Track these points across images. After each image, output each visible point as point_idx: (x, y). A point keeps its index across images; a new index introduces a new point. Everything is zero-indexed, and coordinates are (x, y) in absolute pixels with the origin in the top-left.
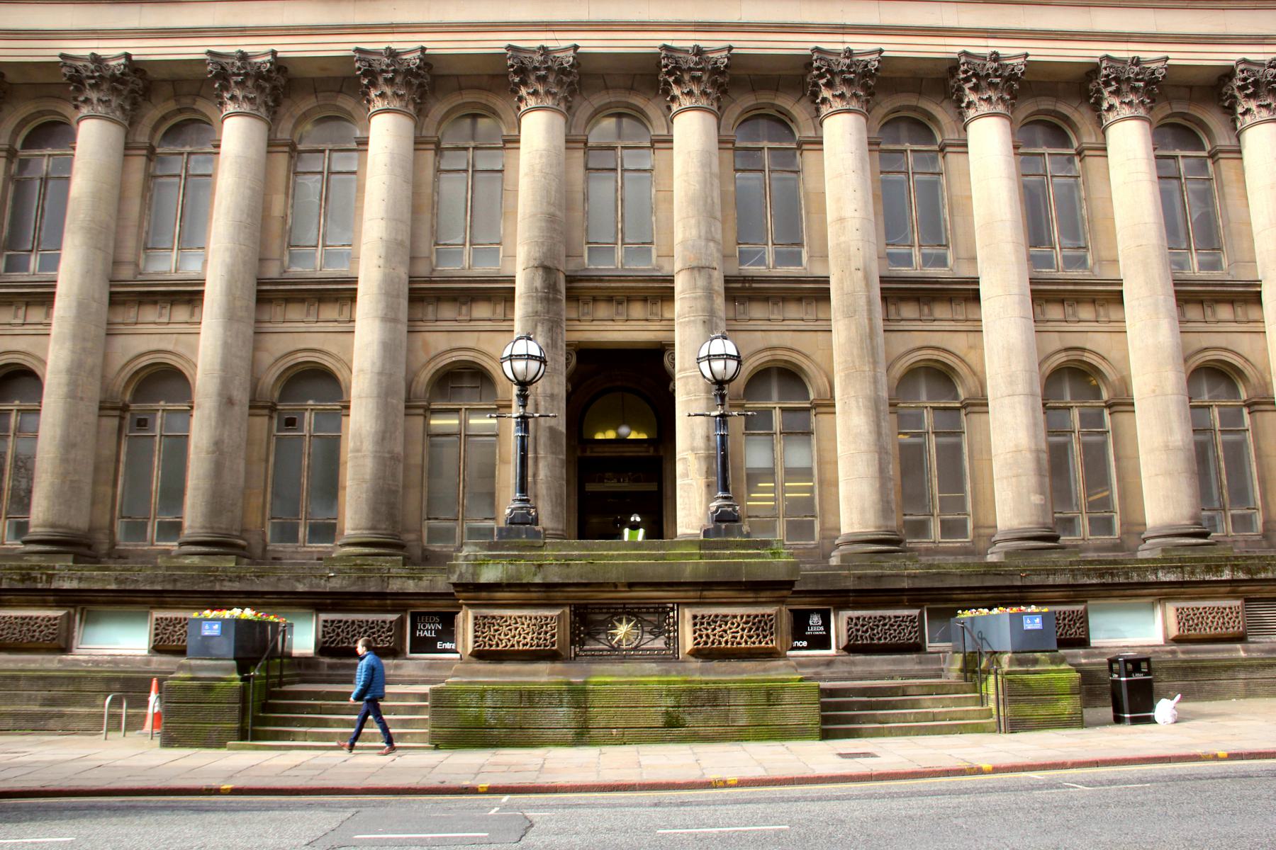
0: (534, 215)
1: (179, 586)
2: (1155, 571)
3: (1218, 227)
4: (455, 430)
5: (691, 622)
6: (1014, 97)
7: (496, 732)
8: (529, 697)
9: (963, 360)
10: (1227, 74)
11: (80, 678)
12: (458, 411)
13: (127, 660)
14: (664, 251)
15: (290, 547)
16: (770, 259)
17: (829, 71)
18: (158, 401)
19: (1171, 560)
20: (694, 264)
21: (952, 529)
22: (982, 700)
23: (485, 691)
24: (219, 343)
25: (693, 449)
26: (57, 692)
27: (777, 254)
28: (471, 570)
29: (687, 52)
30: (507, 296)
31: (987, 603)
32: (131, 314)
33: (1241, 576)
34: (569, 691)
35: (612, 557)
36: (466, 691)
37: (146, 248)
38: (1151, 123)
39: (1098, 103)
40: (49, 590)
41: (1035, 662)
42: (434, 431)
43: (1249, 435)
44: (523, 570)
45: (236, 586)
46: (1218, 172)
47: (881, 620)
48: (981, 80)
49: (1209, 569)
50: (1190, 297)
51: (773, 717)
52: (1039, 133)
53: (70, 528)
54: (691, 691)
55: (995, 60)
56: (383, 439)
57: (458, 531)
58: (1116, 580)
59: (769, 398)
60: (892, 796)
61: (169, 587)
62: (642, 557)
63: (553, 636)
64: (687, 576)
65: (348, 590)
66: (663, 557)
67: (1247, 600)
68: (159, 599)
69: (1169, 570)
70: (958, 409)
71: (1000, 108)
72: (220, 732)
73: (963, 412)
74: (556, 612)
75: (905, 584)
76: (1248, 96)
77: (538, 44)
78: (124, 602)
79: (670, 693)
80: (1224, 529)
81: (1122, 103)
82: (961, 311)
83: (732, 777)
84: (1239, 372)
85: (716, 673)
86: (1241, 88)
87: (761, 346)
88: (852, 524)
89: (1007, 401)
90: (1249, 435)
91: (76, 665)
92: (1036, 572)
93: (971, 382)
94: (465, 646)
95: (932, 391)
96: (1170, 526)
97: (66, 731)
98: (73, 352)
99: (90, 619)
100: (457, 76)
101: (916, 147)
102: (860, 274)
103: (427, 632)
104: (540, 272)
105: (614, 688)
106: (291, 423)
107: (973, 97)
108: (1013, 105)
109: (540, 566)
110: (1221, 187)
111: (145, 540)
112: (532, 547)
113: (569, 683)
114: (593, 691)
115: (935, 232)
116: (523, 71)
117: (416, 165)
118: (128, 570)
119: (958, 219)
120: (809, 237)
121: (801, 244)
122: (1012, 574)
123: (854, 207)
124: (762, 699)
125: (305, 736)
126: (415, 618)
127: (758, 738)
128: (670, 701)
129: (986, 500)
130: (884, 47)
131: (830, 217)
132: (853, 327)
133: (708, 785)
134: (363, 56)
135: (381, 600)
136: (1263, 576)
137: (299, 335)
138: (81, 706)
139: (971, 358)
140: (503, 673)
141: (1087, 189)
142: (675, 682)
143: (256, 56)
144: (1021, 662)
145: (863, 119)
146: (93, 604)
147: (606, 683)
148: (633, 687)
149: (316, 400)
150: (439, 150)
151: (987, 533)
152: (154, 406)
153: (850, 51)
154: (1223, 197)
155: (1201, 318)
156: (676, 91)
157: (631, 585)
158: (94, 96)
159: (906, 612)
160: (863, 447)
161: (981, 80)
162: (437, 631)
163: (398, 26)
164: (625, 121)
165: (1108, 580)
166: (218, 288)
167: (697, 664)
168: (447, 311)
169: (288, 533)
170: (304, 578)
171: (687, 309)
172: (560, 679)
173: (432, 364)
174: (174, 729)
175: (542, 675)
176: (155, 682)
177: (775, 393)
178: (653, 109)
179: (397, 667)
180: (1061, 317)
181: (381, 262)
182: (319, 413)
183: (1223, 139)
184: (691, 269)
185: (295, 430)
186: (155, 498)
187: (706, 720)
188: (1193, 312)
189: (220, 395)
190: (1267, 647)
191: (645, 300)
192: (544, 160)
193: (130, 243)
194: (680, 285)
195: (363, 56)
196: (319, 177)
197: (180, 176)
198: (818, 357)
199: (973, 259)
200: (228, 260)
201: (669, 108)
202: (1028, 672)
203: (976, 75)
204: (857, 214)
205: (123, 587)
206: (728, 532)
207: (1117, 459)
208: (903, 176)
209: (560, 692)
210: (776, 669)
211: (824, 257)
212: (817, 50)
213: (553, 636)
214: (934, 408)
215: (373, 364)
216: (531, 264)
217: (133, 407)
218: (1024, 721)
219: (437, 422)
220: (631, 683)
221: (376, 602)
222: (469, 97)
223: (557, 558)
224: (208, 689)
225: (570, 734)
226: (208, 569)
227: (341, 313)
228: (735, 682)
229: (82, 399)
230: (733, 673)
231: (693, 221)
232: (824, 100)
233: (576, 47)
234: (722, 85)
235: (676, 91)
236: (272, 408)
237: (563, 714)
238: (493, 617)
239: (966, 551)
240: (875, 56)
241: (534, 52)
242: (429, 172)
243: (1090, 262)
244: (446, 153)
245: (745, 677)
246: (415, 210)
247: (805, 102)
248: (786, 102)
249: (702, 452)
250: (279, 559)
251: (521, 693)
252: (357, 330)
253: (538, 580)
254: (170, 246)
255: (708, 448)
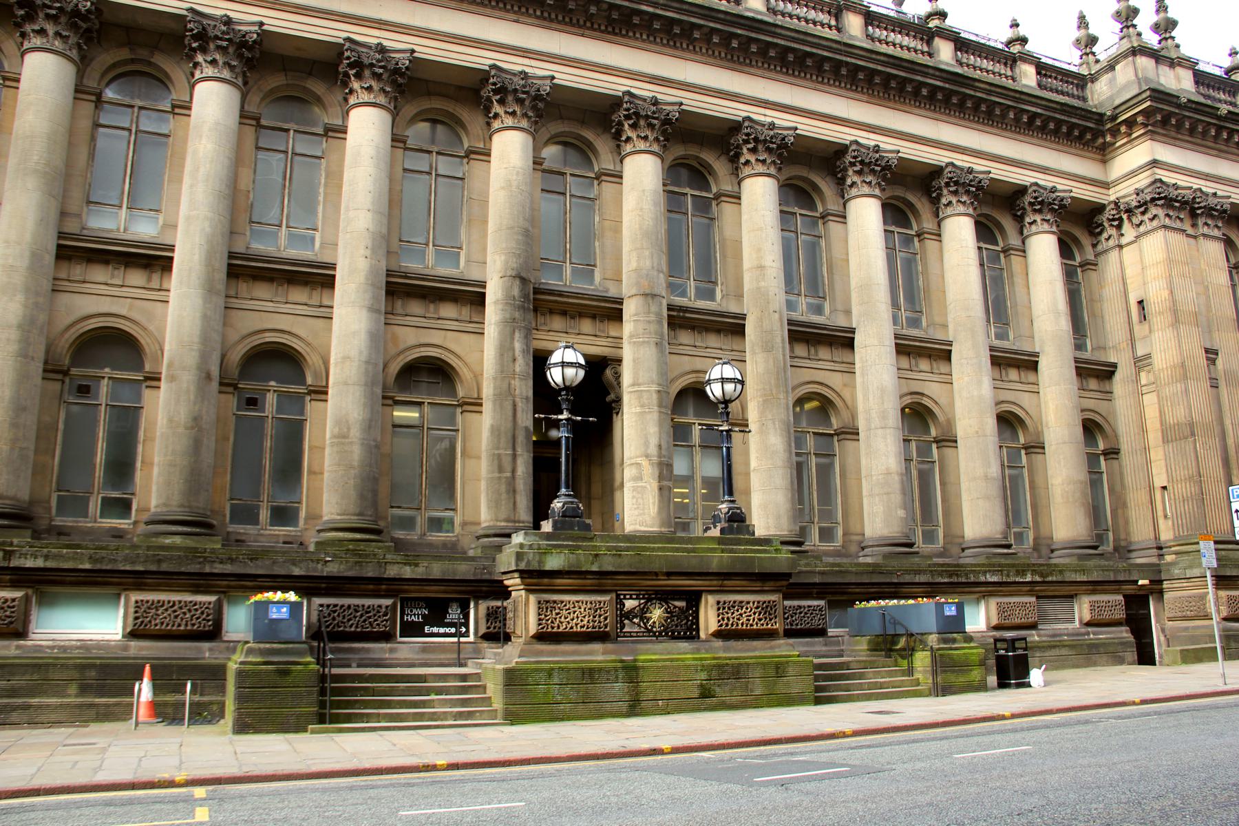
0: (512, 228)
1: (165, 567)
2: (985, 573)
3: (1006, 307)
4: (417, 423)
5: (716, 607)
6: (666, 140)
7: (562, 707)
8: (590, 674)
9: (839, 396)
10: (1021, 190)
11: (47, 665)
12: (420, 404)
13: (100, 645)
14: (609, 275)
15: (250, 529)
16: (692, 291)
17: (637, 114)
18: (102, 368)
19: (994, 566)
20: (648, 291)
21: (826, 534)
22: (910, 671)
23: (553, 669)
24: (198, 315)
25: (647, 456)
26: (17, 681)
27: (697, 288)
28: (537, 558)
29: (645, 100)
30: (479, 300)
31: (864, 597)
32: (78, 271)
33: (1038, 579)
34: (624, 668)
35: (653, 549)
36: (536, 670)
37: (89, 202)
38: (778, 180)
39: (843, 179)
40: (8, 568)
41: (954, 641)
42: (397, 422)
43: (1025, 471)
44: (582, 558)
45: (228, 568)
46: (1009, 264)
47: (816, 609)
48: (758, 143)
49: (1018, 573)
50: (906, 349)
51: (781, 688)
52: (684, 173)
53: (18, 500)
54: (719, 666)
55: (654, 105)
56: (370, 427)
57: (419, 519)
58: (960, 580)
59: (686, 415)
60: (1047, 726)
61: (153, 568)
62: (677, 550)
63: (606, 619)
64: (714, 567)
65: (346, 574)
66: (694, 550)
67: (1038, 597)
68: (138, 580)
69: (993, 572)
70: (832, 435)
71: (656, 148)
72: (299, 716)
73: (836, 438)
74: (607, 598)
75: (817, 580)
76: (1035, 211)
77: (519, 68)
78: (96, 583)
79: (703, 668)
80: (814, 541)
81: (757, 160)
82: (840, 354)
83: (848, 728)
84: (1021, 421)
85: (736, 651)
86: (1031, 204)
87: (688, 368)
88: (768, 528)
89: (880, 432)
90: (1025, 471)
91: (39, 651)
92: (908, 572)
93: (845, 415)
94: (527, 629)
95: (820, 422)
96: (1074, 541)
97: (33, 724)
98: (26, 306)
99: (47, 601)
100: (427, 81)
101: (803, 212)
102: (777, 315)
103: (415, 616)
104: (518, 282)
105: (660, 664)
106: (252, 402)
107: (856, 179)
108: (665, 146)
109: (597, 555)
110: (1011, 276)
111: (86, 516)
112: (585, 539)
113: (622, 661)
114: (643, 667)
115: (815, 287)
116: (358, 65)
117: (73, 116)
118: (102, 548)
119: (837, 278)
120: (603, 259)
121: (715, 283)
122: (890, 573)
123: (772, 258)
124: (772, 672)
125: (378, 718)
126: (403, 600)
127: (770, 705)
128: (703, 675)
129: (853, 510)
130: (556, 75)
131: (747, 264)
132: (771, 361)
133: (832, 736)
134: (353, 47)
135: (379, 586)
136: (1050, 579)
137: (275, 315)
138: (48, 697)
139: (846, 394)
140: (564, 653)
141: (925, 265)
142: (706, 659)
143: (241, 24)
144: (945, 641)
145: (530, 139)
146: (52, 585)
147: (652, 661)
148: (675, 663)
149: (113, 369)
150: (259, 126)
151: (955, 539)
152: (98, 372)
153: (526, 73)
154: (1012, 284)
155: (907, 367)
156: (356, 85)
157: (669, 575)
158: (51, 29)
159: (815, 603)
160: (780, 463)
161: (758, 143)
162: (424, 616)
163: (386, 23)
164: (440, 128)
165: (955, 579)
166: (196, 257)
167: (719, 643)
168: (416, 307)
169: (246, 514)
170: (301, 561)
171: (641, 331)
172: (613, 657)
173: (402, 357)
174: (249, 715)
175: (597, 654)
176: (148, 668)
177: (691, 411)
178: (473, 120)
179: (391, 650)
180: (907, 367)
181: (368, 253)
182: (281, 395)
183: (833, 205)
184: (645, 295)
185: (255, 410)
186: (99, 472)
187: (732, 690)
188: (801, 350)
189: (199, 368)
190: (1051, 632)
191: (594, 317)
192: (520, 178)
193: (77, 195)
194: (630, 309)
195: (353, 47)
196: (282, 155)
197: (130, 130)
198: (471, 358)
199: (848, 312)
200: (208, 230)
201: (346, 100)
202: (951, 649)
203: (862, 162)
204: (774, 265)
205: (98, 566)
206: (739, 531)
207: (943, 484)
208: (792, 234)
209: (616, 669)
210: (779, 646)
211: (739, 296)
212: (629, 93)
213: (606, 619)
214: (814, 433)
215: (361, 352)
216: (509, 273)
217: (74, 371)
218: (950, 687)
219: (400, 414)
220: (672, 660)
221: (371, 587)
222: (437, 104)
223: (608, 549)
224: (285, 673)
225: (624, 706)
226: (195, 550)
227: (310, 297)
228: (751, 658)
229: (33, 358)
230: (748, 650)
231: (647, 253)
232: (496, 116)
233: (553, 78)
234: (400, 85)
235: (356, 85)
236: (235, 387)
237: (619, 688)
238: (555, 602)
239: (837, 554)
240: (791, 132)
241: (514, 75)
242: (85, 124)
243: (924, 324)
244: (106, 106)
245: (757, 653)
246: (390, 202)
247: (607, 137)
248: (709, 157)
249: (655, 459)
250: (243, 541)
251: (583, 671)
252: (335, 316)
253: (595, 568)
254: (116, 202)
255: (660, 456)
